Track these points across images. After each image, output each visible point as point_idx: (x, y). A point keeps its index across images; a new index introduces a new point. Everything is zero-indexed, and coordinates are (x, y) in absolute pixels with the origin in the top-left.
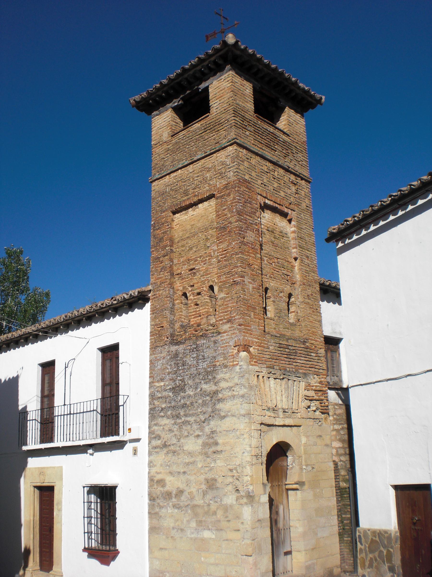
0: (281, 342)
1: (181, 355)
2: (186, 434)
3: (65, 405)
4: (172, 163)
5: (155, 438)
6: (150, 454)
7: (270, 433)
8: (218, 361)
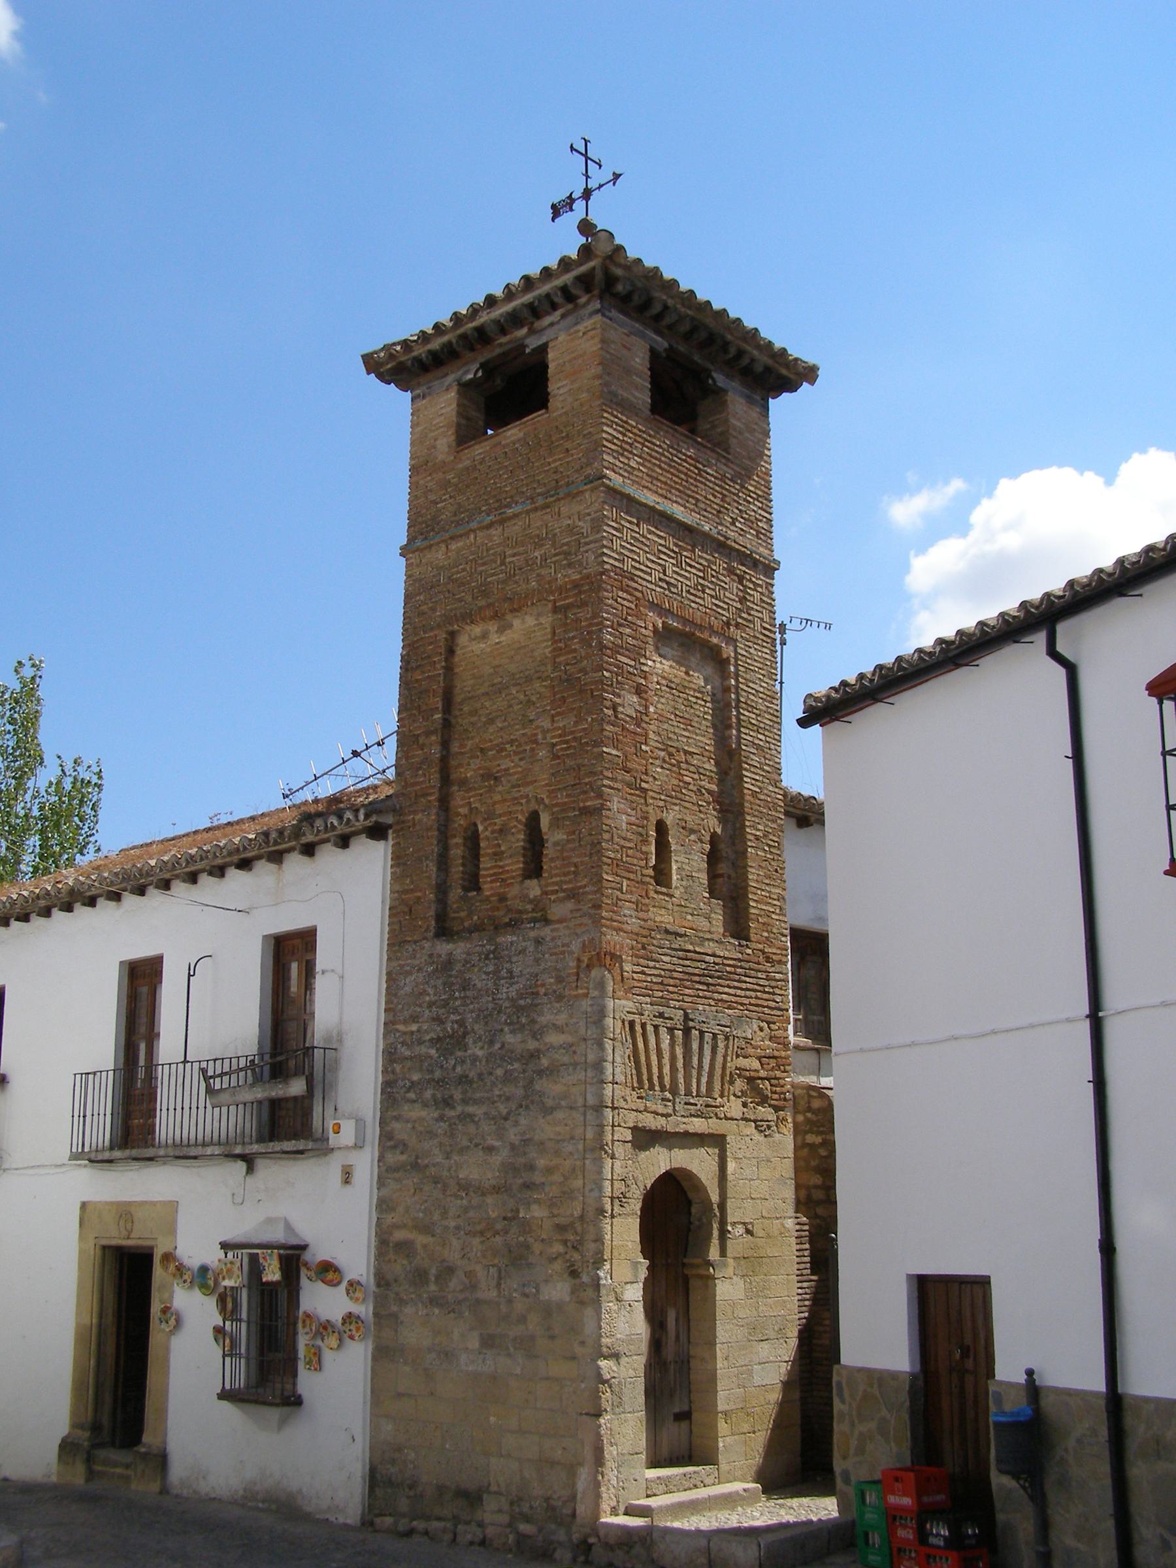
1: (458, 967)
2: (465, 1143)
3: (185, 1062)
4: (455, 515)
5: (395, 1147)
6: (381, 1183)
8: (543, 985)
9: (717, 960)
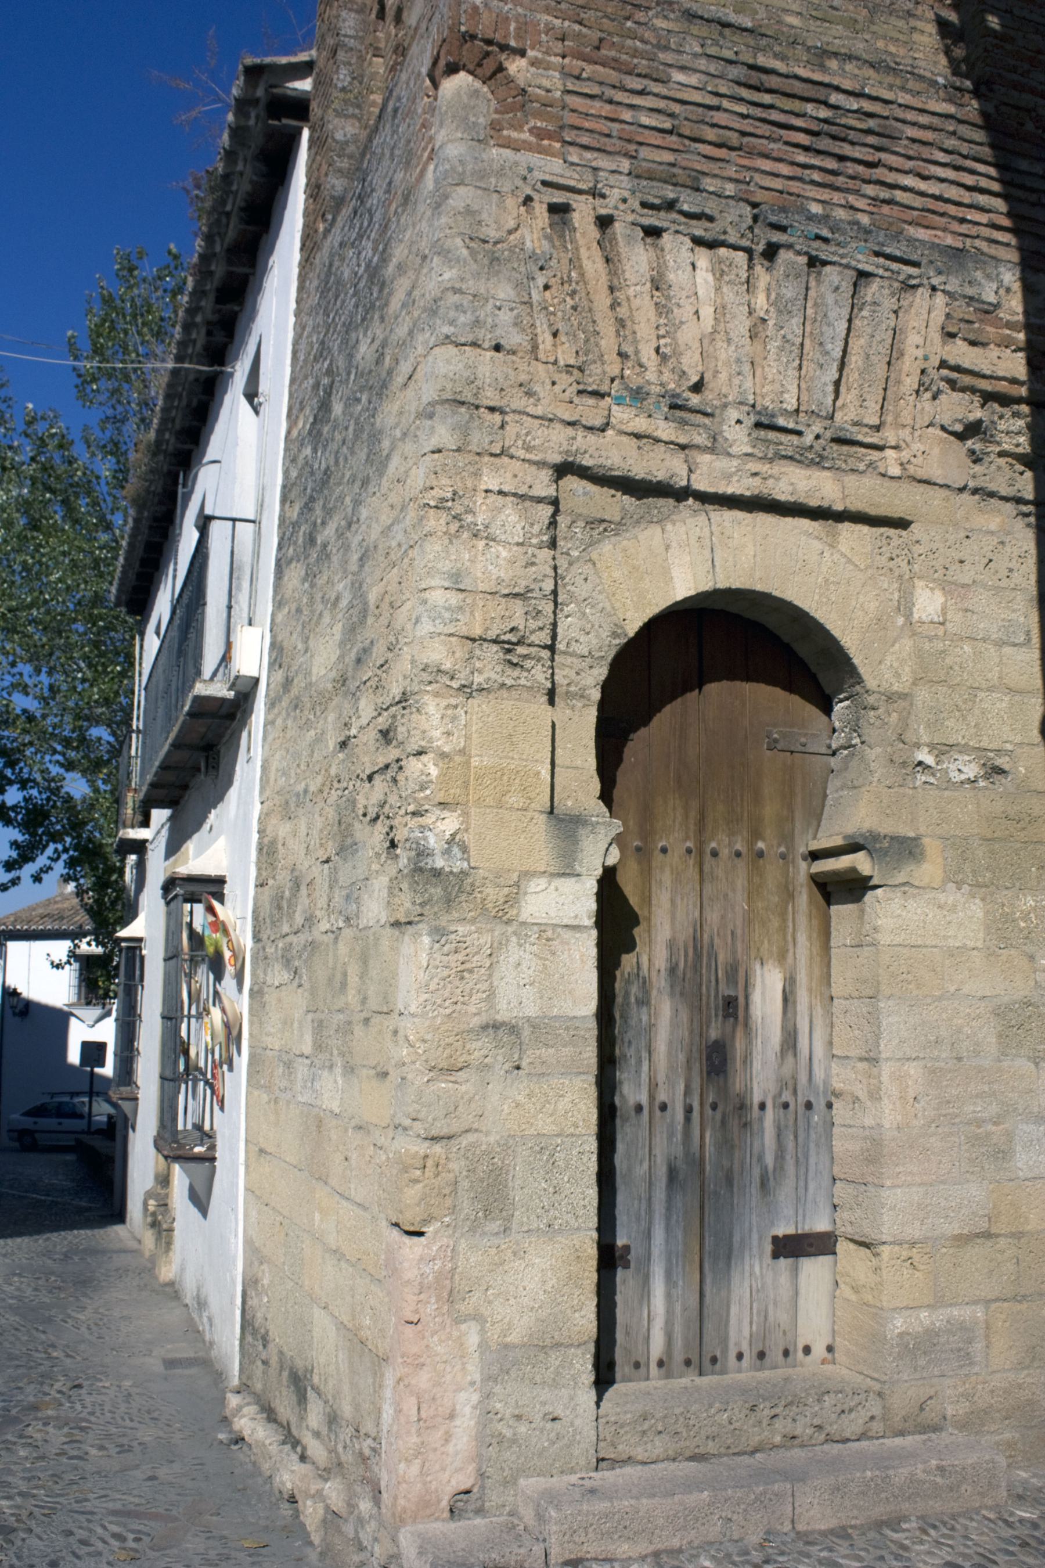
0: (762, 60)
7: (650, 537)
9: (868, 106)
